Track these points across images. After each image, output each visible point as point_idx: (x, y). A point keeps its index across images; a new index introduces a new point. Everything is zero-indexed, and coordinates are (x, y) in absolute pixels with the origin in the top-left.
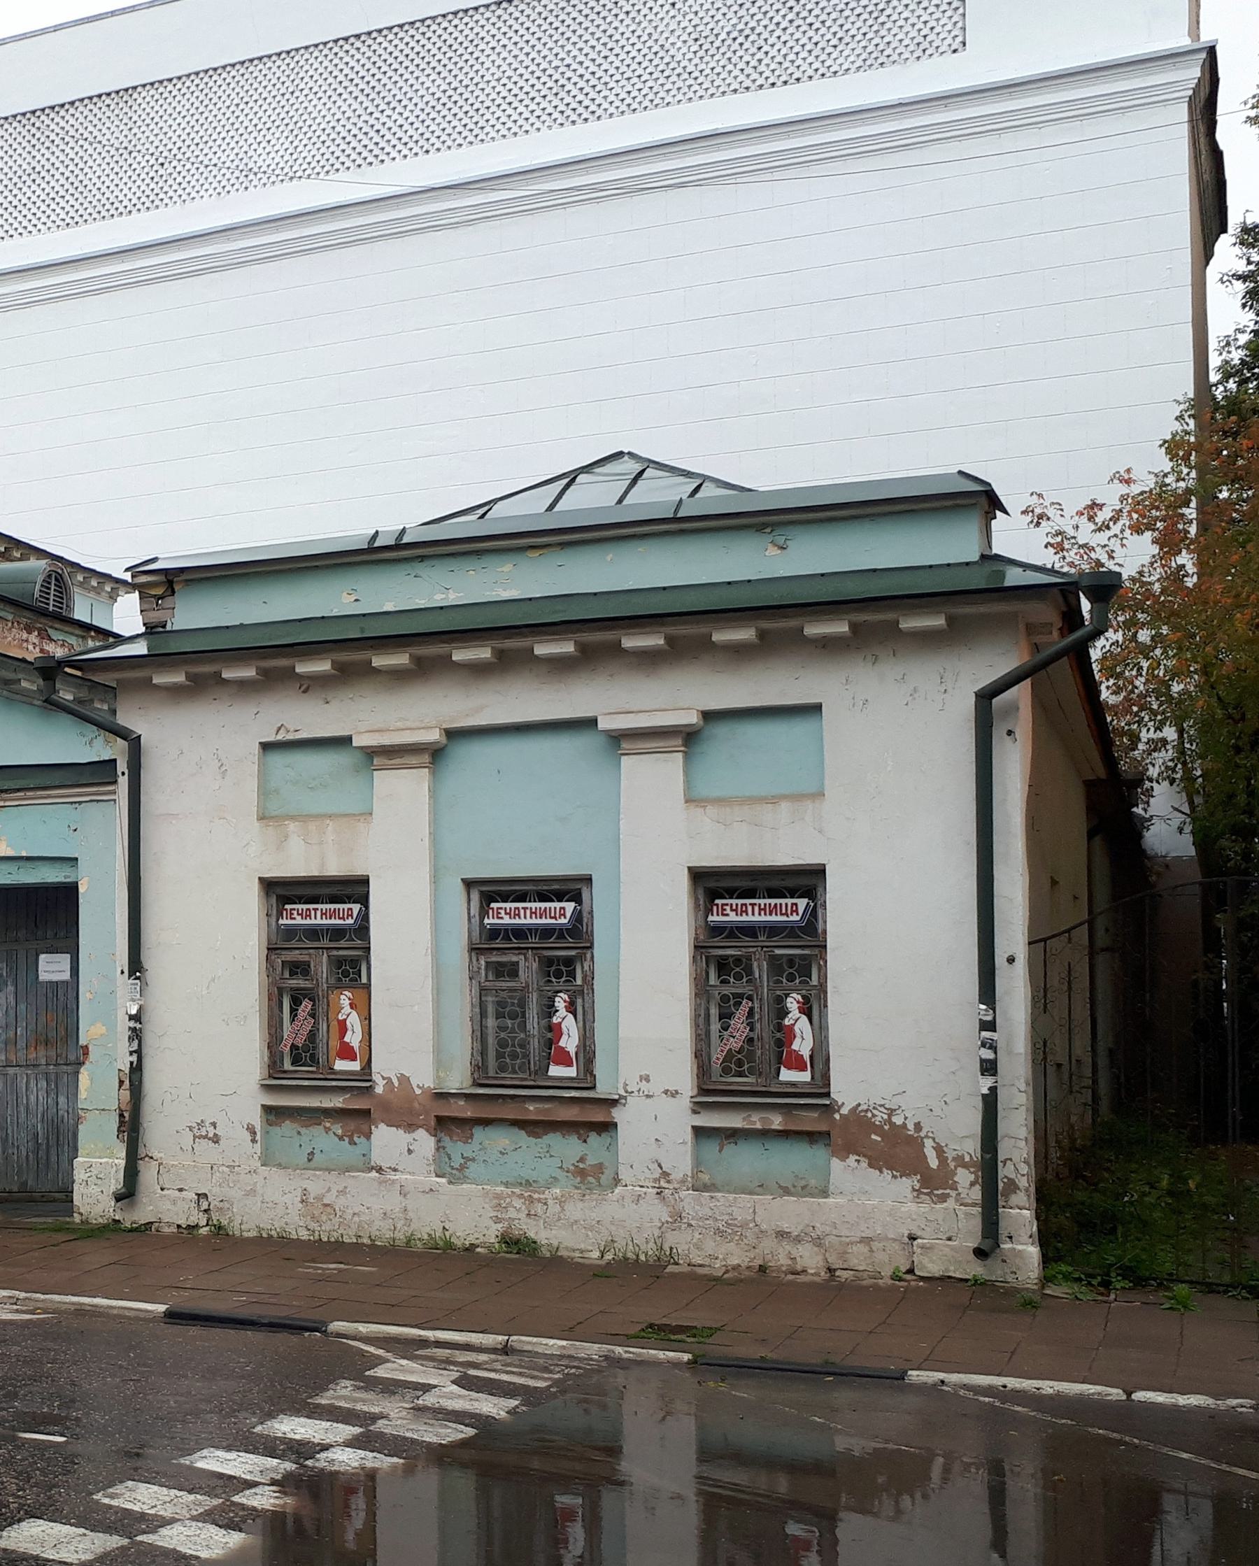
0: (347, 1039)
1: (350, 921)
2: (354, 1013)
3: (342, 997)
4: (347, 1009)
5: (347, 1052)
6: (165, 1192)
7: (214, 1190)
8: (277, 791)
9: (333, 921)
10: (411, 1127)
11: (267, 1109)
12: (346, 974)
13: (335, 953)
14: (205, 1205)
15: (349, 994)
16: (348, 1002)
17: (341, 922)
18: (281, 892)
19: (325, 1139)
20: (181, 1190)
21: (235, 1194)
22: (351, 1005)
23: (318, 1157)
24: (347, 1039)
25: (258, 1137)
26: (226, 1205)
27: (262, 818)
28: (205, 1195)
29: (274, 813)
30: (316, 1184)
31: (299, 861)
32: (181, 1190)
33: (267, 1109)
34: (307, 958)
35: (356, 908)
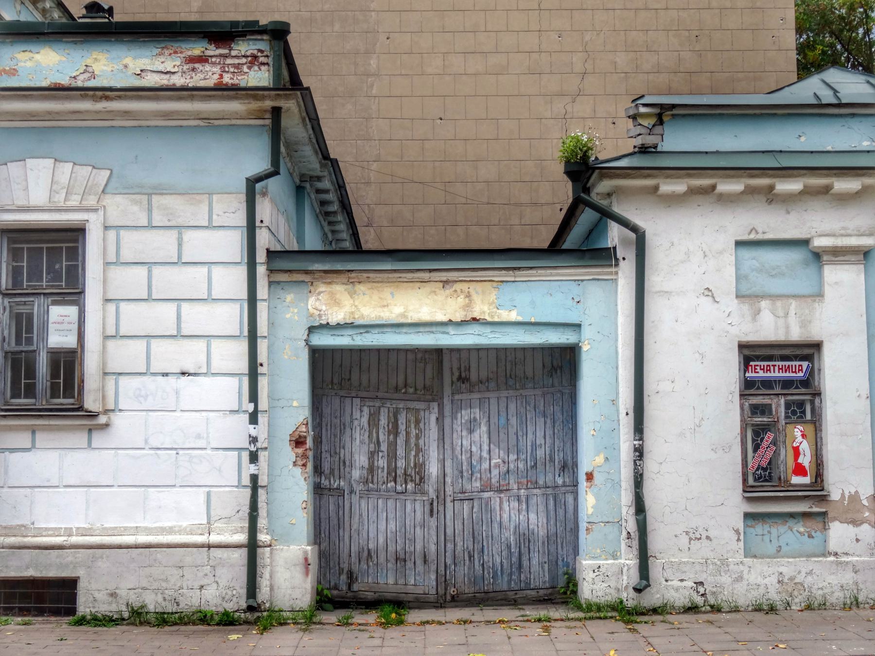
0: (800, 461)
1: (801, 374)
2: (805, 442)
3: (796, 430)
4: (800, 439)
5: (800, 470)
6: (669, 583)
7: (709, 579)
8: (746, 277)
9: (787, 374)
10: (855, 523)
11: (747, 516)
12: (794, 413)
13: (790, 398)
14: (701, 590)
15: (802, 428)
16: (800, 434)
17: (794, 375)
18: (751, 353)
19: (791, 535)
20: (682, 580)
21: (725, 579)
22: (803, 436)
23: (785, 549)
24: (800, 461)
25: (742, 537)
26: (719, 590)
27: (737, 297)
28: (701, 583)
29: (744, 293)
30: (787, 567)
31: (769, 327)
32: (682, 580)
33: (747, 516)
34: (769, 402)
35: (805, 364)
